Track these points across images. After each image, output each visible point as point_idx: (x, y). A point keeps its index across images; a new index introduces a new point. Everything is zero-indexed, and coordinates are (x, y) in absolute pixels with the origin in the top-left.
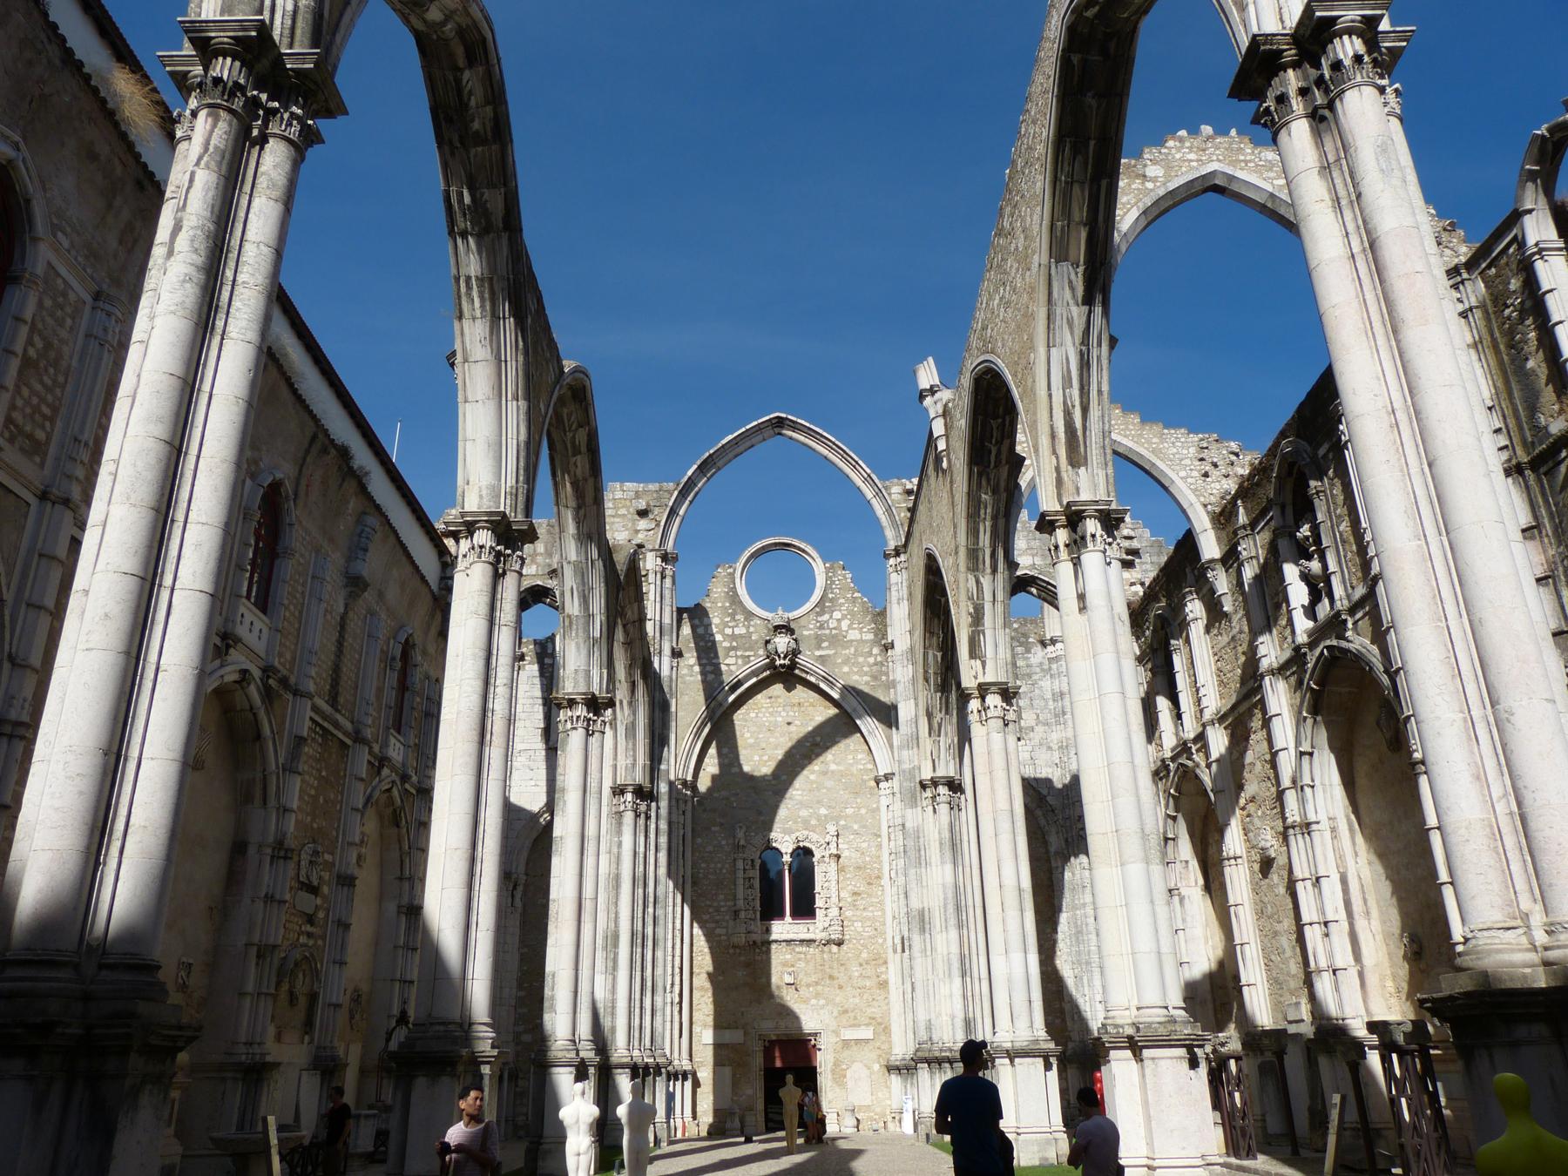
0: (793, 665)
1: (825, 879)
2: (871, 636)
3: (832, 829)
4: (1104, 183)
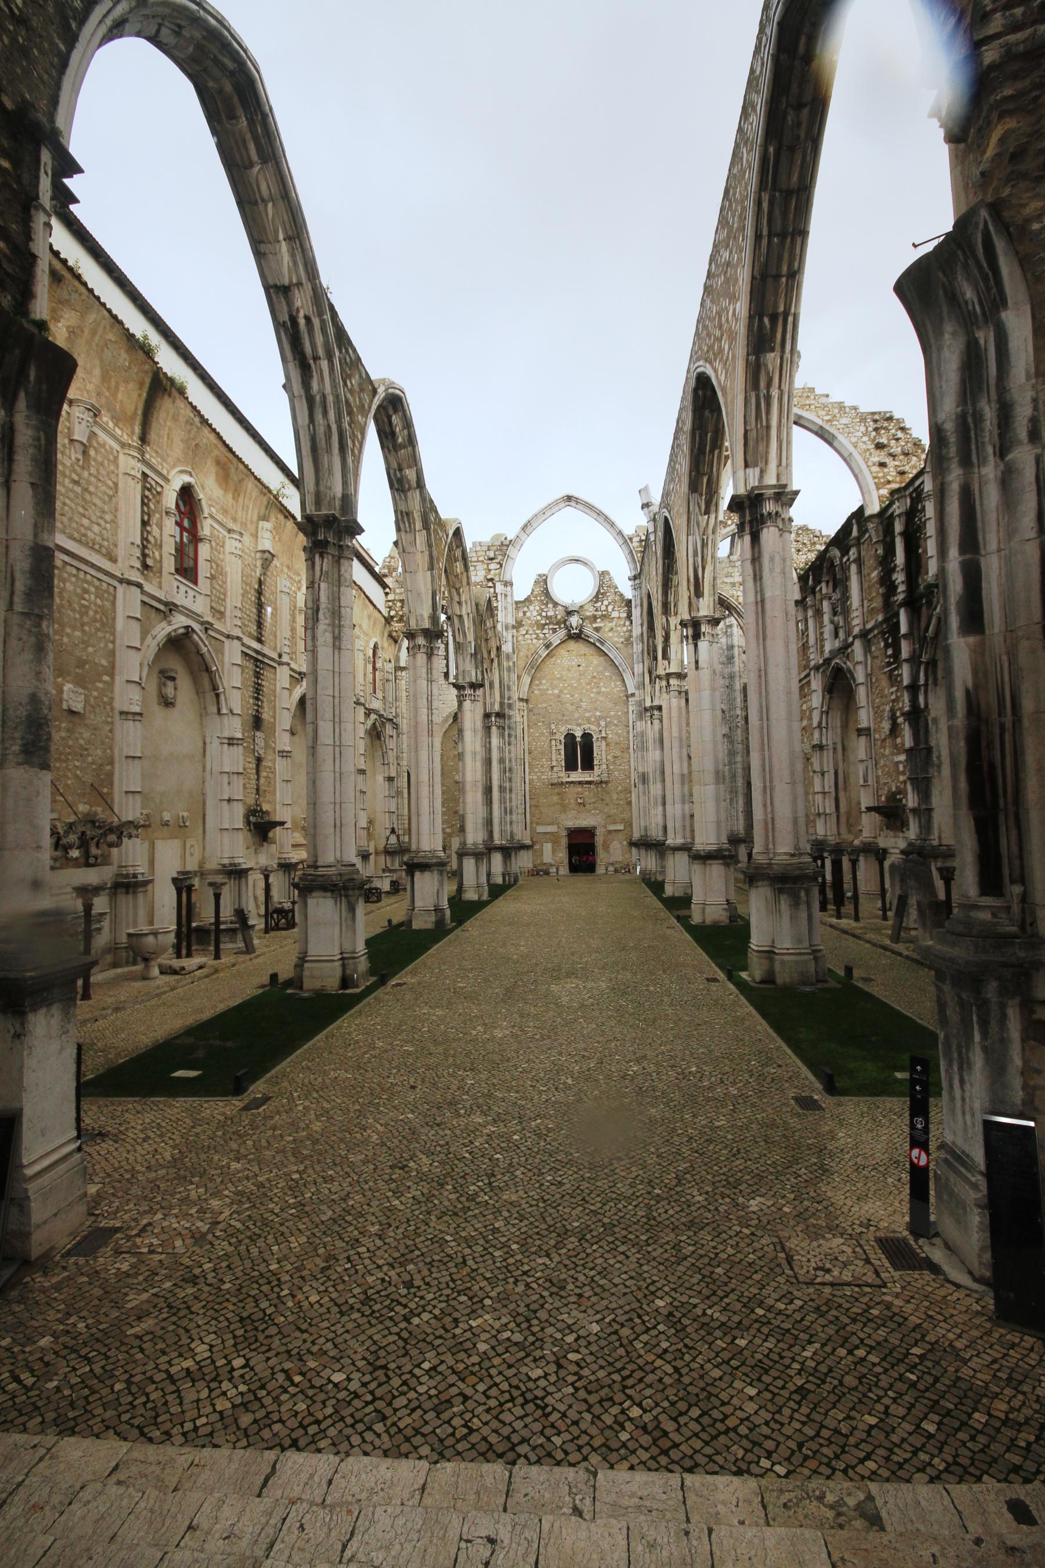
0: (581, 631)
1: (600, 751)
3: (603, 723)
4: (716, 452)
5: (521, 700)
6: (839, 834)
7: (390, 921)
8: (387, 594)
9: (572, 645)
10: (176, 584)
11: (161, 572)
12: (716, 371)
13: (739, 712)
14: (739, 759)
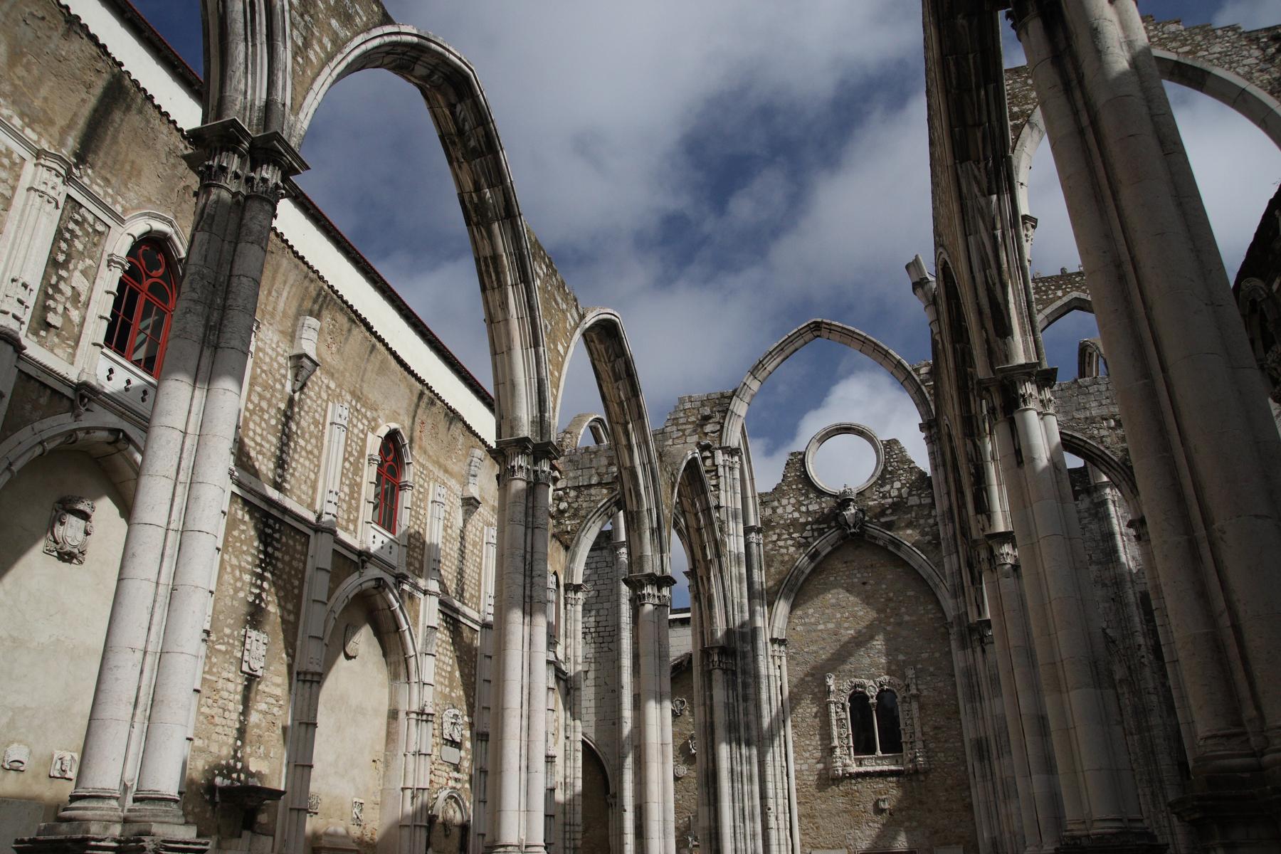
1: (910, 719)
3: (910, 673)
11: (77, 342)
13: (1141, 640)
14: (1155, 720)
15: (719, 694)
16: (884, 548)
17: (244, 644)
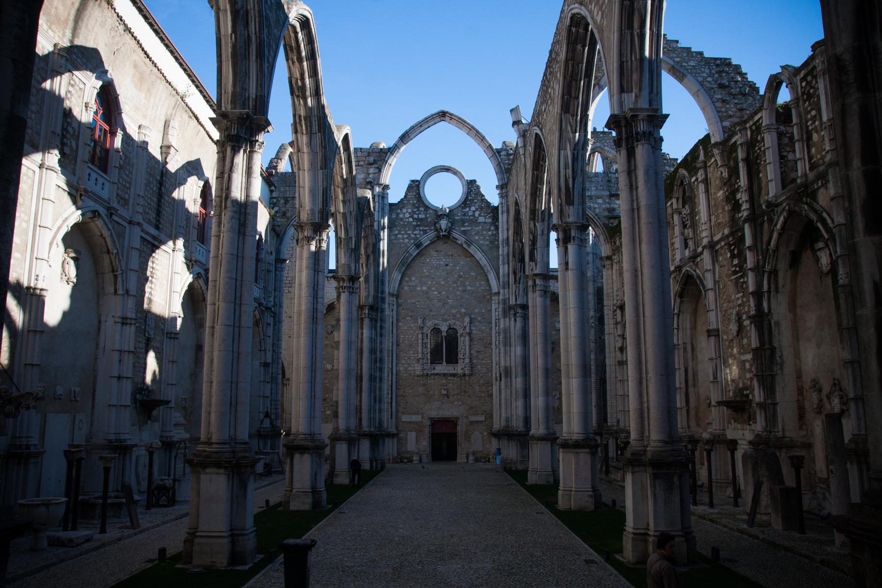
1: (464, 344)
2: (490, 220)
3: (467, 319)
5: (393, 295)
6: (689, 427)
7: (267, 502)
8: (271, 191)
9: (441, 246)
10: (88, 171)
12: (590, 12)
15: (366, 332)
16: (461, 245)
17: (145, 321)
